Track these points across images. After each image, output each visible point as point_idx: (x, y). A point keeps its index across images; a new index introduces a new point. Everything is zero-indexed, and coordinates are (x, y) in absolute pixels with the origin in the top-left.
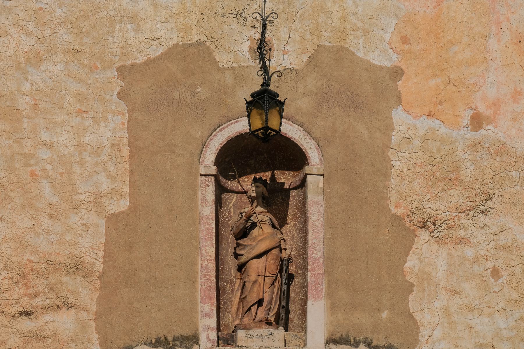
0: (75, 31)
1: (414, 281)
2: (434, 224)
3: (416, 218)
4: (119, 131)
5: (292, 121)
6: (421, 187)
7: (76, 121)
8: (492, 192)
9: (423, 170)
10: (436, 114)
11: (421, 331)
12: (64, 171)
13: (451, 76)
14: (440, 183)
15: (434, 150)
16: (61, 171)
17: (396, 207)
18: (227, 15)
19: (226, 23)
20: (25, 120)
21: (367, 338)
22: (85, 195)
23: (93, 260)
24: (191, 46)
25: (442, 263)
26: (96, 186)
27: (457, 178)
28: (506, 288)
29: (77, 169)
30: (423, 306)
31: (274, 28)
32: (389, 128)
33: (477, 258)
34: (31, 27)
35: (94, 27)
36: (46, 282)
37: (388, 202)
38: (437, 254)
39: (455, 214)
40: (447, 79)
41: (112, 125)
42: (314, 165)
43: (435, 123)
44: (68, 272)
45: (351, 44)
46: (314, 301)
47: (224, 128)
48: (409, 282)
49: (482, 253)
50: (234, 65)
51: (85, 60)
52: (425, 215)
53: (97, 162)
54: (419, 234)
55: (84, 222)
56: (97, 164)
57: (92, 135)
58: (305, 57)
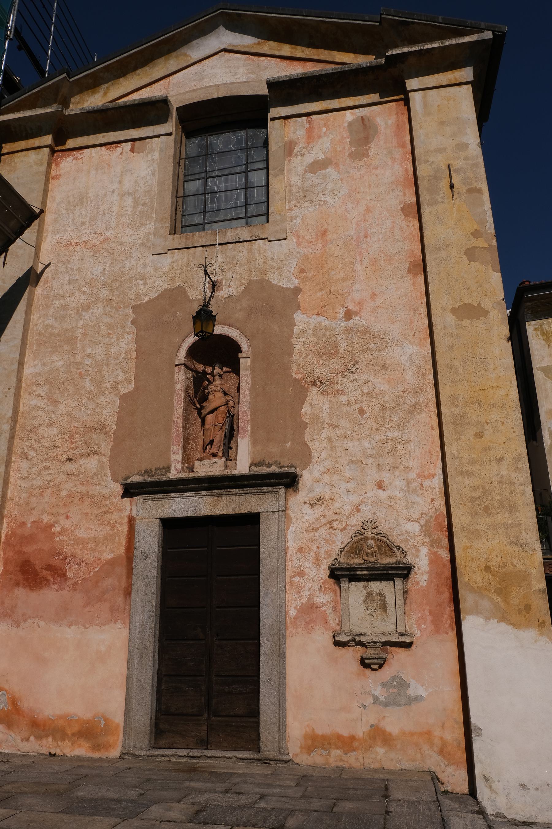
2: (321, 382)
3: (308, 380)
7: (106, 340)
8: (359, 359)
16: (96, 370)
20: (79, 343)
21: (277, 461)
24: (175, 289)
25: (326, 408)
26: (116, 378)
27: (335, 352)
28: (369, 421)
29: (105, 368)
31: (224, 273)
32: (292, 324)
33: (349, 403)
34: (86, 289)
36: (83, 439)
37: (291, 371)
39: (334, 375)
41: (127, 340)
43: (321, 319)
49: (352, 398)
55: (107, 400)
56: (117, 364)
57: (115, 348)
58: (242, 288)
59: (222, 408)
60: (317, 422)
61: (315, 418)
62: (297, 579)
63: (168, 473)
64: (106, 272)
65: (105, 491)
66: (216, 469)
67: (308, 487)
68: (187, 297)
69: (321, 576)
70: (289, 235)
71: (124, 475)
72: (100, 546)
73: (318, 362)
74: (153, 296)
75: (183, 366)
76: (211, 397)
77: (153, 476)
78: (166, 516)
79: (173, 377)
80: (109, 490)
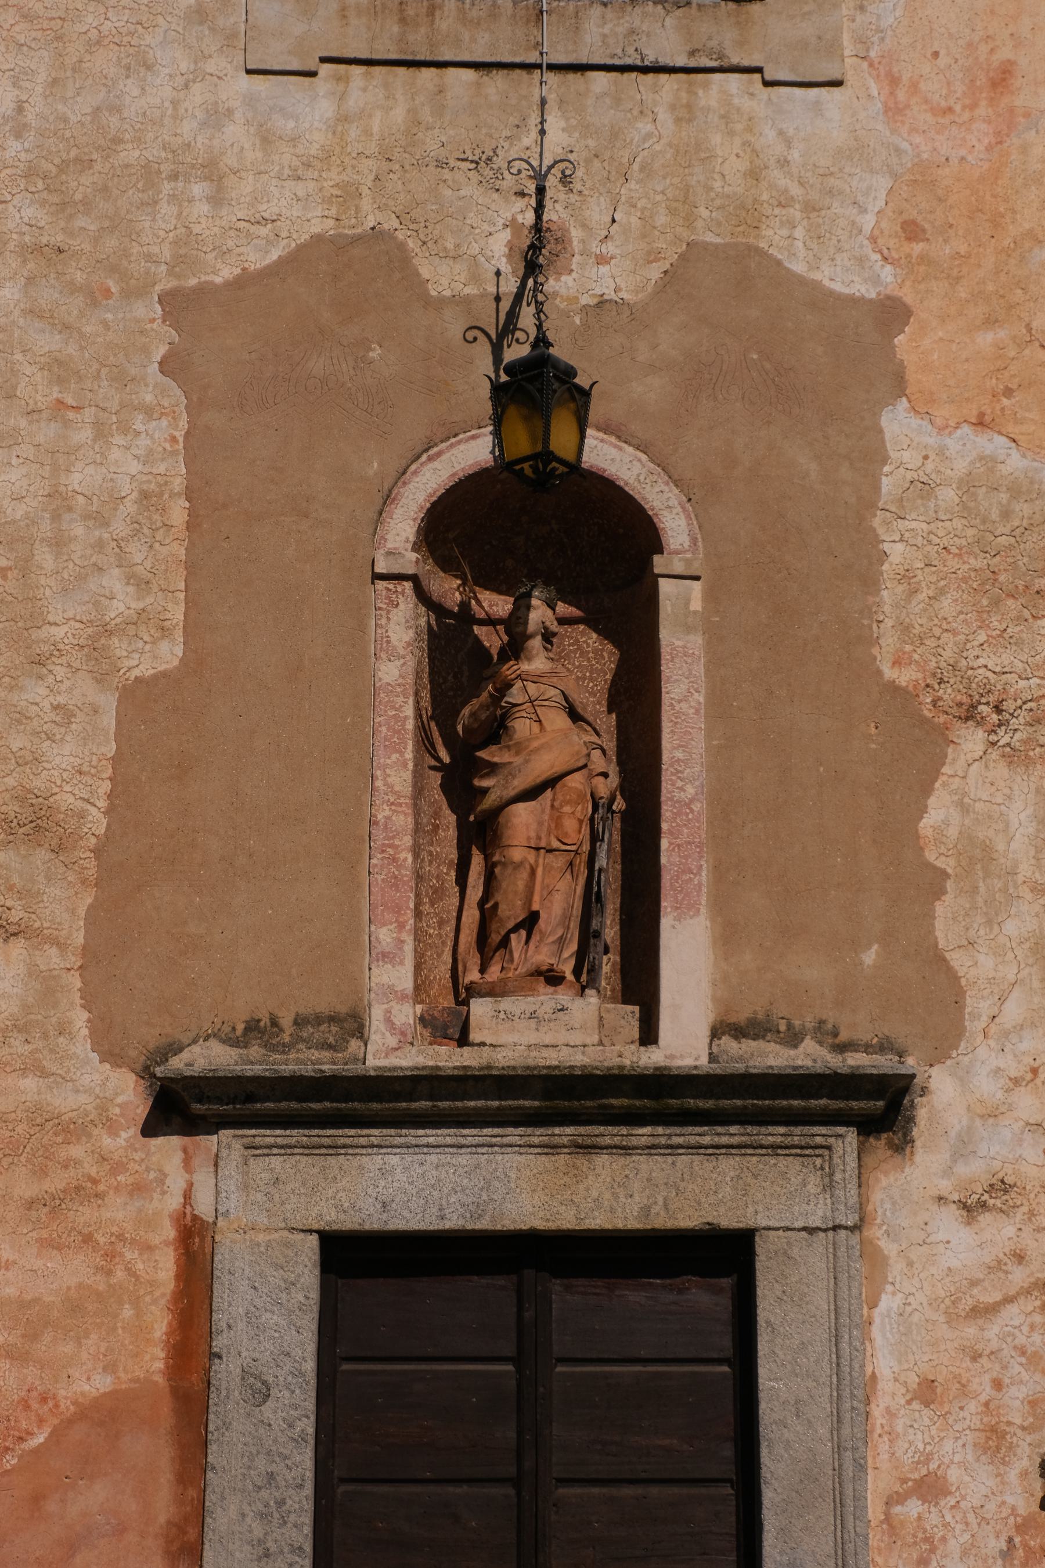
0: (55, 199)
1: (947, 864)
2: (998, 709)
3: (948, 694)
4: (163, 460)
5: (619, 437)
6: (961, 612)
7: (47, 432)
9: (967, 566)
10: (997, 420)
11: (969, 1001)
12: (10, 563)
13: (1034, 325)
14: (1010, 602)
15: (995, 515)
17: (896, 663)
18: (452, 163)
19: (450, 183)
21: (822, 1022)
22: (64, 629)
23: (80, 804)
24: (357, 239)
25: (1021, 816)
26: (96, 604)
29: (45, 558)
30: (972, 933)
31: (574, 198)
32: (873, 455)
35: (105, 189)
37: (875, 651)
38: (1007, 791)
40: (1024, 331)
41: (143, 442)
42: (677, 552)
43: (995, 444)
44: (11, 838)
45: (773, 238)
46: (678, 919)
47: (439, 454)
48: (935, 867)
50: (467, 290)
51: (79, 273)
52: (974, 685)
53: (100, 538)
54: (959, 737)
55: (61, 699)
56: (100, 545)
57: (90, 470)
58: (655, 273)
59: (575, 781)
60: (987, 874)
61: (978, 856)
62: (913, 1508)
63: (354, 1044)
64: (30, 116)
65: (66, 1101)
66: (563, 1037)
67: (953, 1134)
68: (416, 285)
69: (1010, 1500)
70: (850, 67)
71: (152, 1037)
72: (47, 1337)
73: (983, 625)
74: (257, 260)
75: (408, 585)
76: (521, 726)
77: (285, 1048)
78: (348, 1222)
79: (362, 628)
80: (83, 1098)
